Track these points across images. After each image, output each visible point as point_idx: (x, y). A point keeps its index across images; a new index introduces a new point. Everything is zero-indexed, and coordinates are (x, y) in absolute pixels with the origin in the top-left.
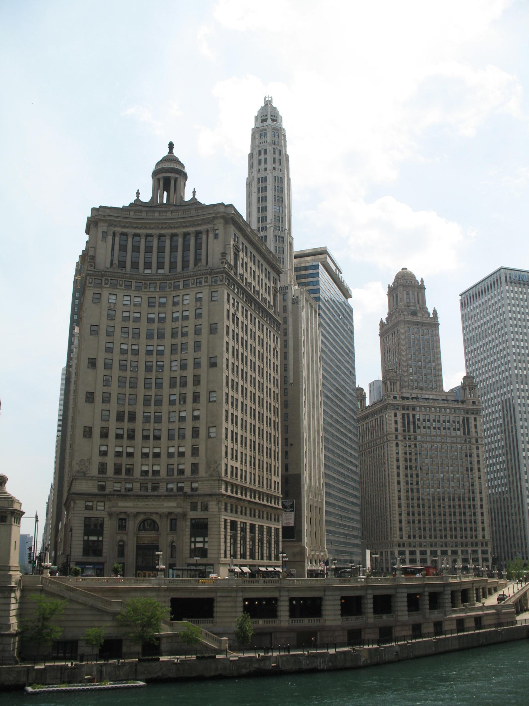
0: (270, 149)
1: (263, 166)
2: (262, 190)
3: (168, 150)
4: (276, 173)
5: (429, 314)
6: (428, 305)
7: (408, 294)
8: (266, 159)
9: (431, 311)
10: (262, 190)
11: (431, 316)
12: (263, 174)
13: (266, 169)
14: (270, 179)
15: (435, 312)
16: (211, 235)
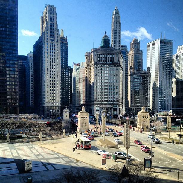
0: (117, 22)
1: (115, 27)
2: (116, 33)
3: (105, 33)
4: (119, 29)
5: (140, 51)
6: (140, 49)
7: (136, 45)
8: (116, 25)
9: (141, 50)
10: (116, 33)
11: (141, 51)
12: (115, 29)
13: (116, 28)
14: (117, 31)
15: (142, 50)
16: (116, 56)
